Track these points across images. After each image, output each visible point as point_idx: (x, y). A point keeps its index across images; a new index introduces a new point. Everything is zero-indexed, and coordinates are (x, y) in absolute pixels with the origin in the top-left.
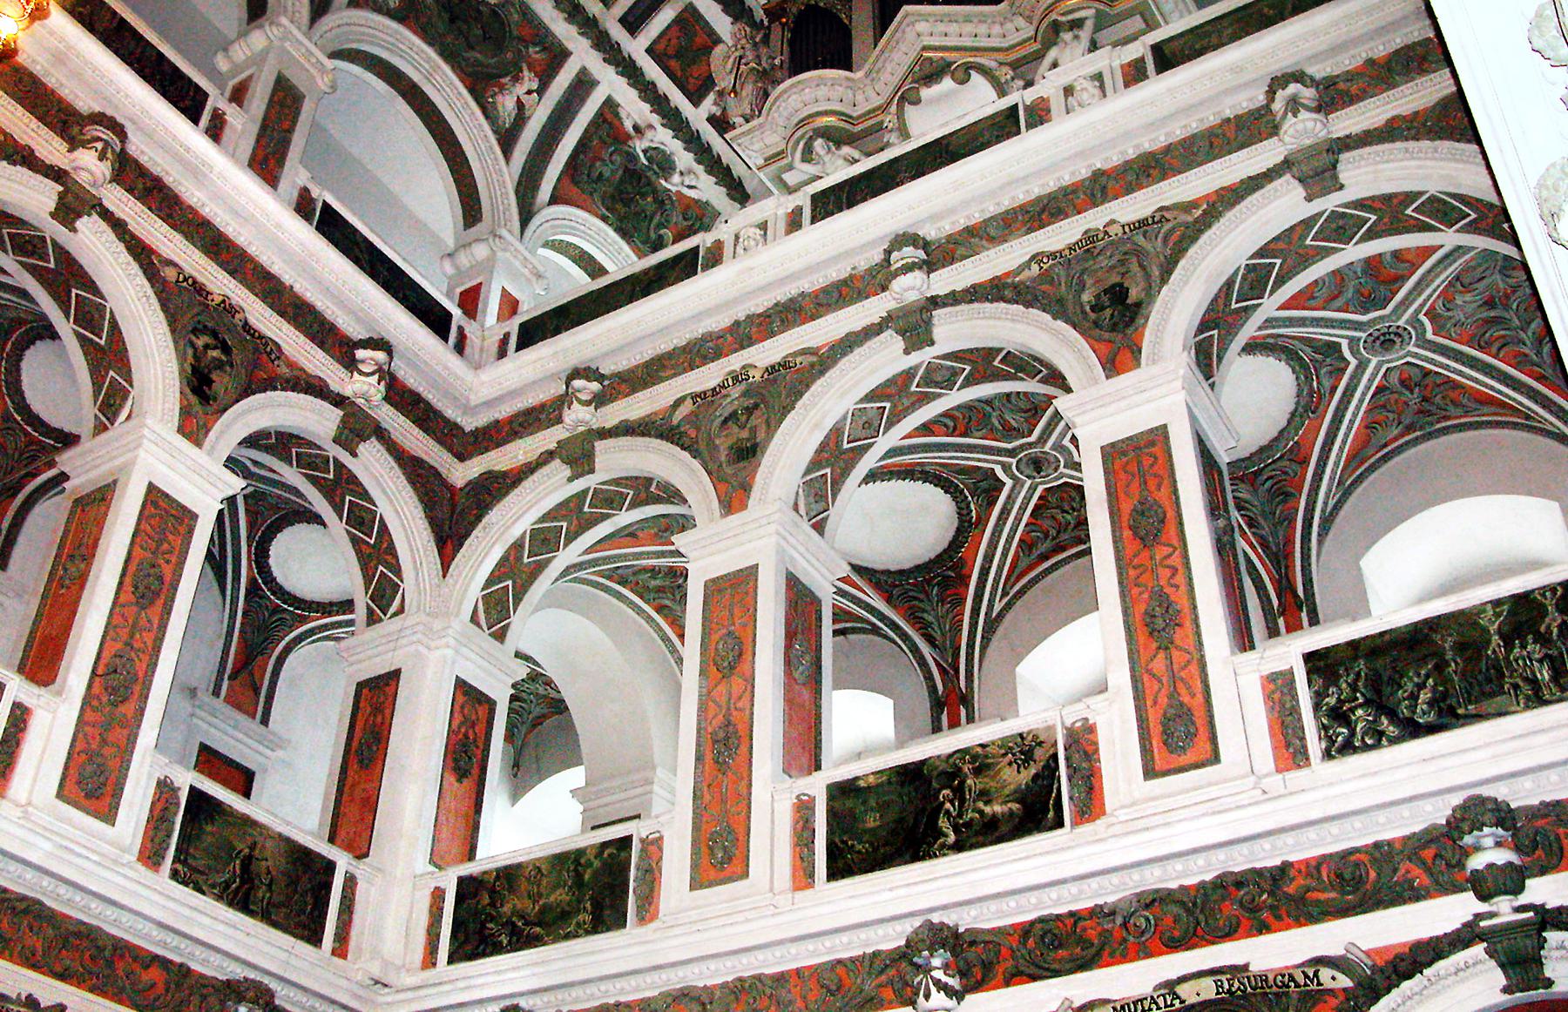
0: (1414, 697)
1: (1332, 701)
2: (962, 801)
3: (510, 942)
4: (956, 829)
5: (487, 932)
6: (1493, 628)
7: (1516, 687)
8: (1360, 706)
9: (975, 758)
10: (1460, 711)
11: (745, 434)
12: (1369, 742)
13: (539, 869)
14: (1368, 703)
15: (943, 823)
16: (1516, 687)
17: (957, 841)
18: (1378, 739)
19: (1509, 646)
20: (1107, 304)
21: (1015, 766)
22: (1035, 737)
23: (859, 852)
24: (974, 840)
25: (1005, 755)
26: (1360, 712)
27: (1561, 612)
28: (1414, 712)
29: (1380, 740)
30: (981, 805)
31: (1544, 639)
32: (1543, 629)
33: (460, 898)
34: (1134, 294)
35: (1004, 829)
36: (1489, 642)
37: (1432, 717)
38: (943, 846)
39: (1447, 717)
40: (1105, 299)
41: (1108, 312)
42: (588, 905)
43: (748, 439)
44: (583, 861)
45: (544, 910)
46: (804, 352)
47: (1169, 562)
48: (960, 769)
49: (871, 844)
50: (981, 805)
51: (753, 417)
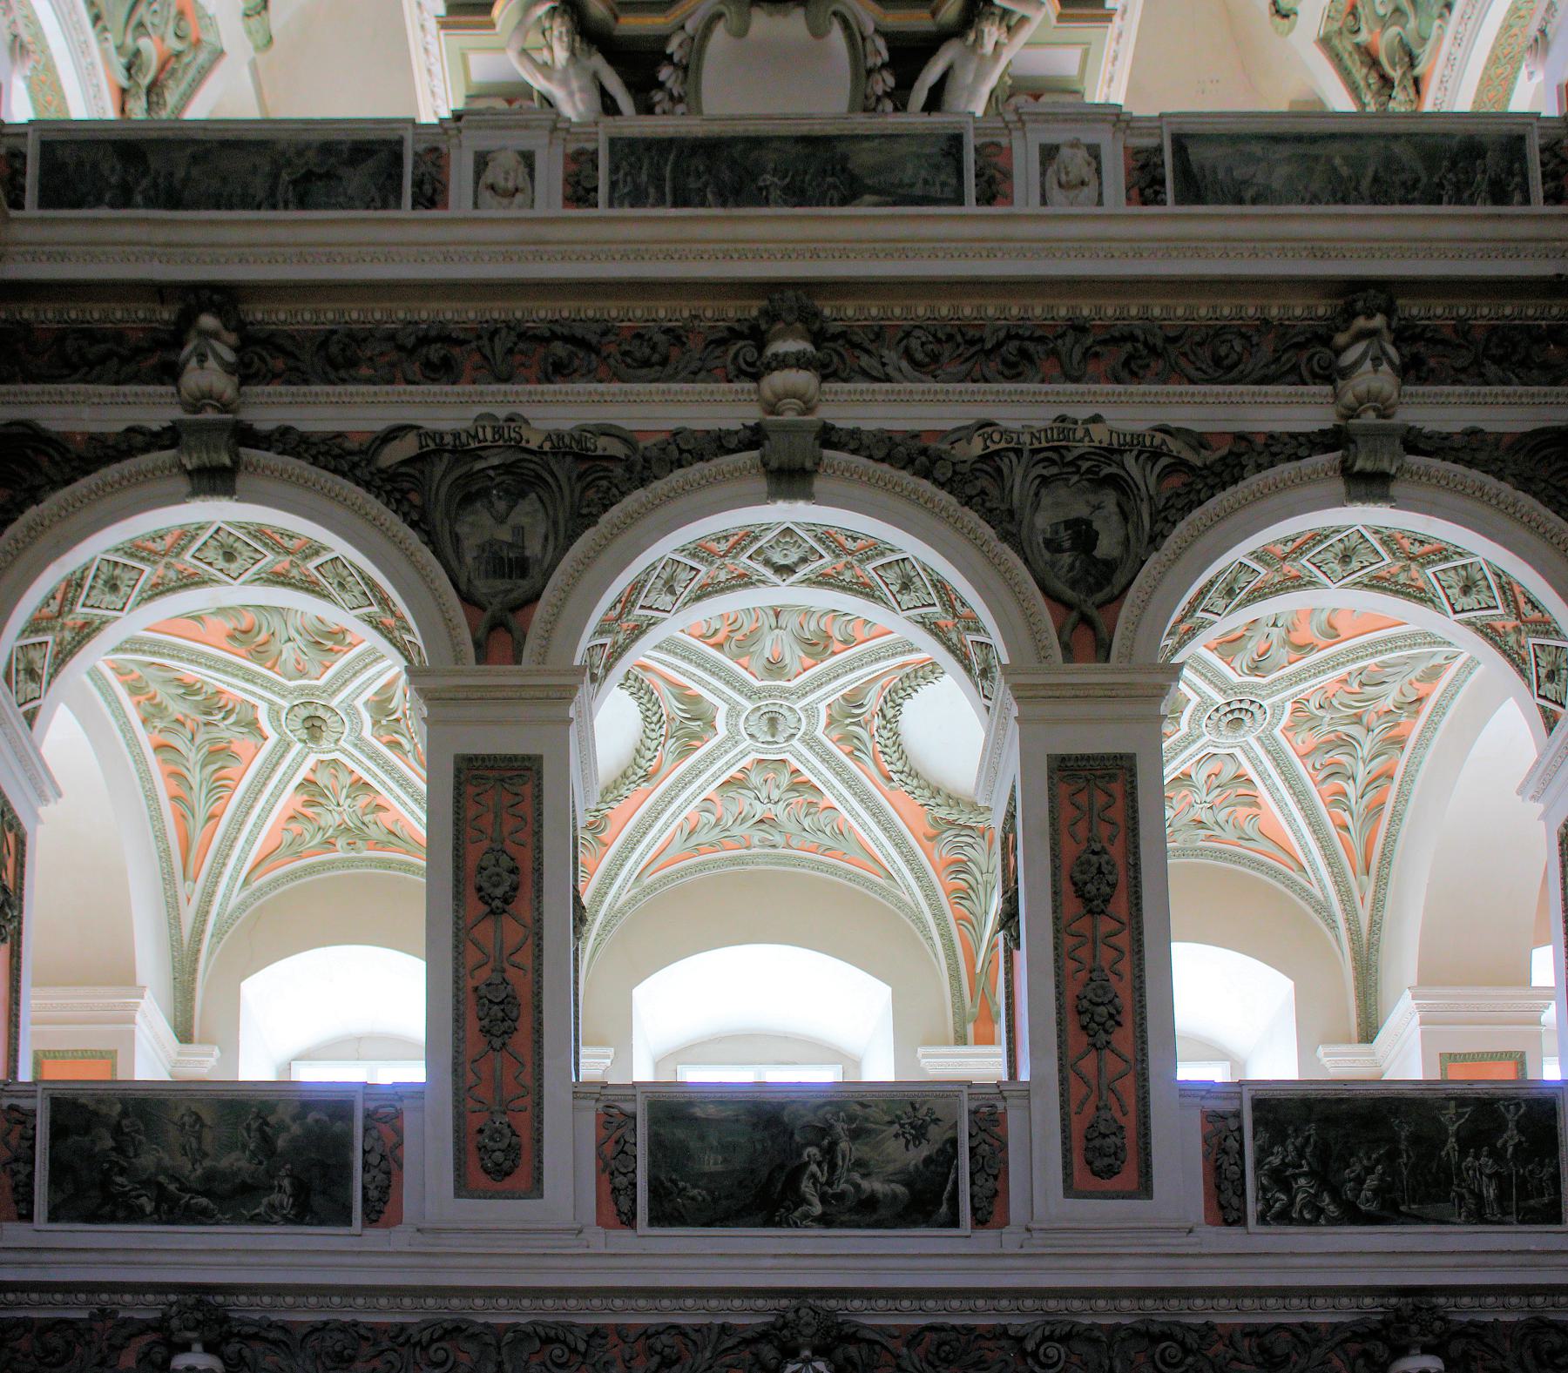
0: (1360, 1181)
1: (1276, 1161)
2: (833, 1167)
3: (157, 1209)
4: (824, 1199)
5: (115, 1189)
6: (1452, 1129)
7: (1461, 1197)
8: (1304, 1175)
9: (851, 1118)
10: (1403, 1208)
11: (505, 534)
12: (1307, 1216)
13: (199, 1118)
14: (1310, 1174)
15: (806, 1187)
16: (1461, 1197)
17: (824, 1214)
18: (1317, 1216)
19: (1463, 1153)
20: (1067, 545)
21: (902, 1141)
22: (930, 1111)
23: (693, 1199)
24: (845, 1218)
25: (891, 1123)
26: (1302, 1181)
27: (1521, 1130)
28: (1358, 1197)
29: (1318, 1217)
30: (856, 1176)
31: (1497, 1155)
32: (1499, 1144)
33: (58, 1132)
34: (1107, 546)
35: (883, 1213)
36: (1445, 1142)
37: (1373, 1207)
38: (806, 1216)
39: (1388, 1212)
40: (1065, 536)
41: (1066, 558)
42: (286, 1183)
43: (511, 546)
44: (272, 1119)
45: (210, 1176)
46: (607, 431)
47: (1114, 940)
48: (831, 1126)
49: (711, 1192)
50: (856, 1176)
51: (517, 509)
